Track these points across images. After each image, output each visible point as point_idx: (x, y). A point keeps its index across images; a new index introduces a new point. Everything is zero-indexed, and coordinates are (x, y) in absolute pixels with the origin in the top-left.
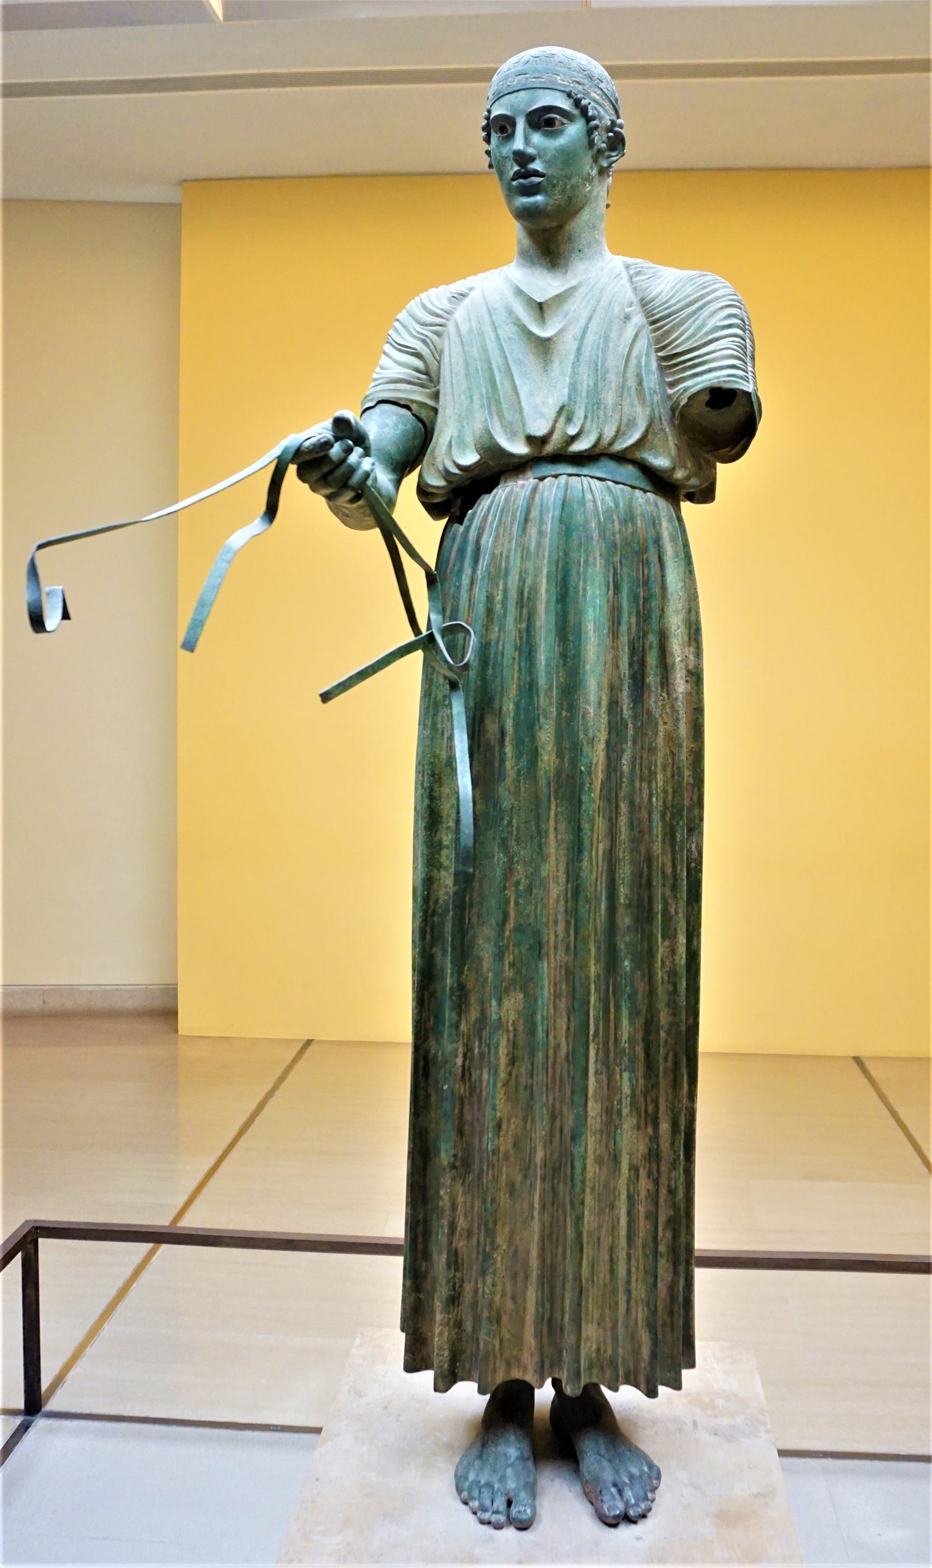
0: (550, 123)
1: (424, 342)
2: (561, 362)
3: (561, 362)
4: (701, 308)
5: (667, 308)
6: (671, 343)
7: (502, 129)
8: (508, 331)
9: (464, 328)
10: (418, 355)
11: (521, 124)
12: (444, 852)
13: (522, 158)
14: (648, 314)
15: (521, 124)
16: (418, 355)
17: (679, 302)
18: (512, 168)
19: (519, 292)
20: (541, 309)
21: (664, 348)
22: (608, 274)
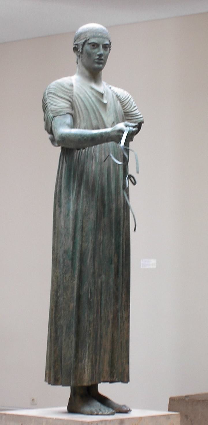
0: (106, 47)
1: (70, 97)
2: (109, 110)
3: (109, 110)
4: (129, 101)
5: (123, 99)
6: (126, 108)
7: (93, 46)
8: (93, 99)
9: (81, 96)
10: (70, 101)
11: (101, 47)
12: (84, 238)
13: (100, 55)
14: (120, 100)
15: (101, 47)
16: (70, 101)
17: (125, 97)
18: (96, 56)
19: (92, 88)
20: (102, 95)
21: (124, 109)
22: (110, 88)
